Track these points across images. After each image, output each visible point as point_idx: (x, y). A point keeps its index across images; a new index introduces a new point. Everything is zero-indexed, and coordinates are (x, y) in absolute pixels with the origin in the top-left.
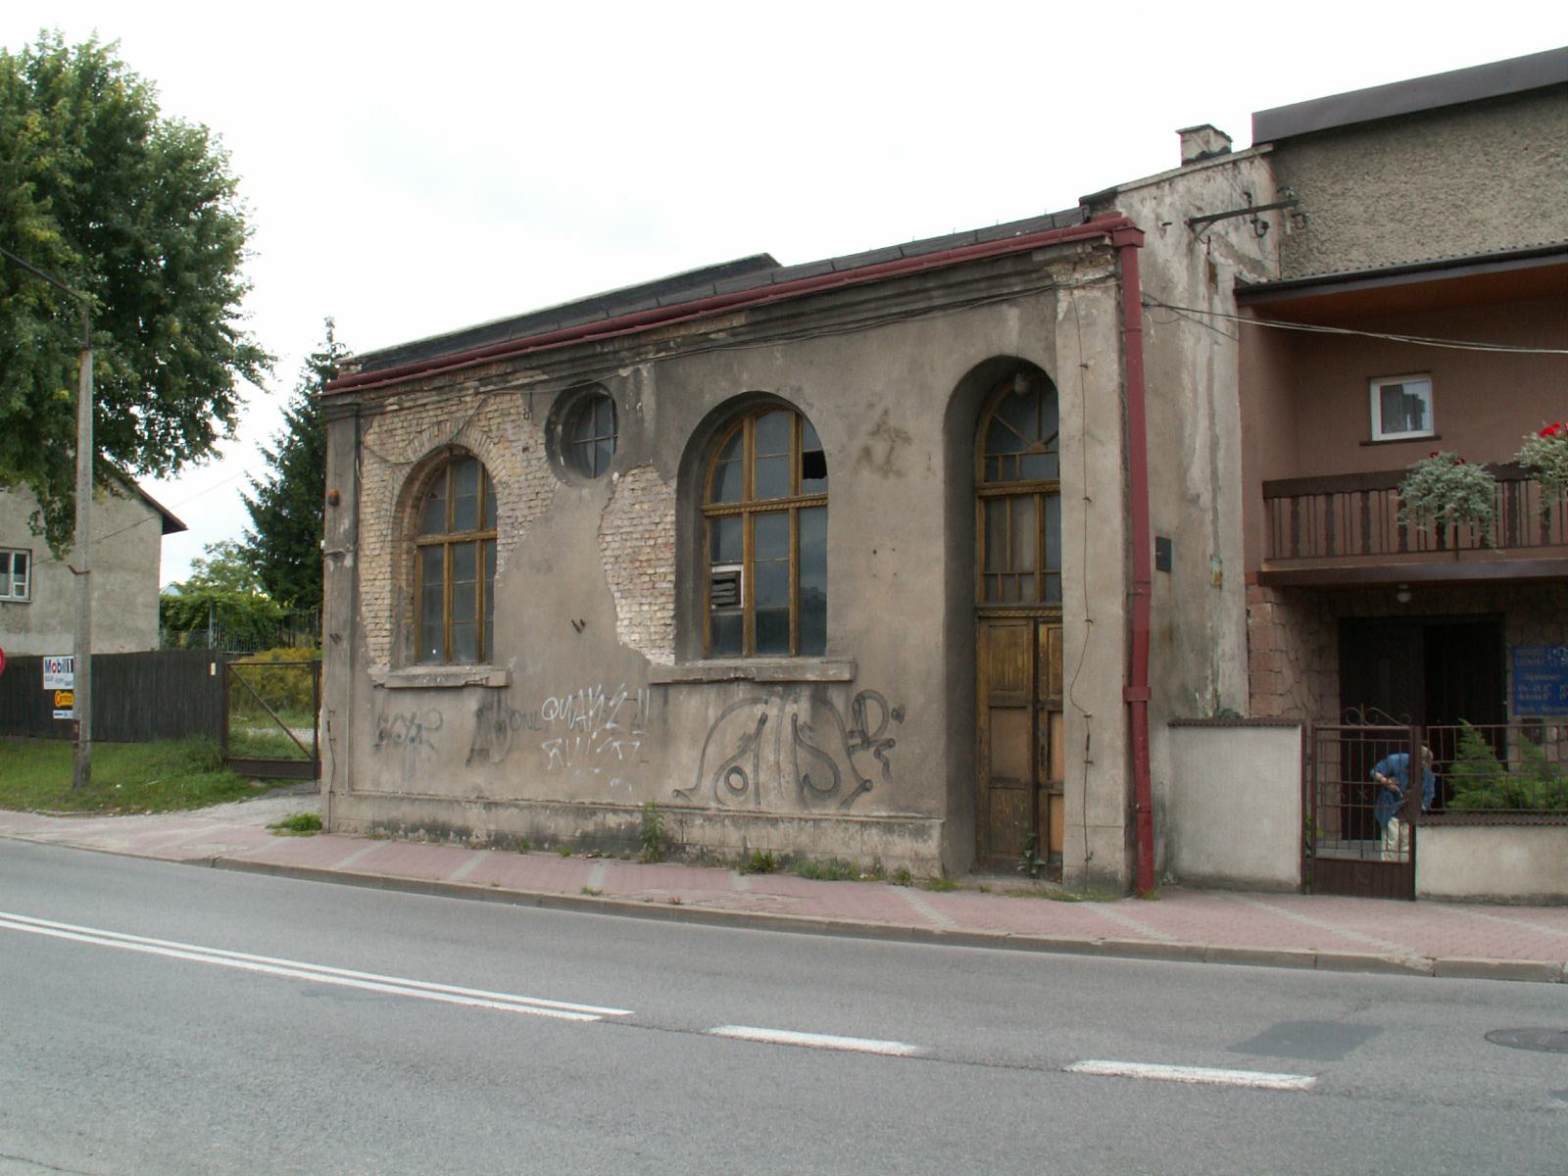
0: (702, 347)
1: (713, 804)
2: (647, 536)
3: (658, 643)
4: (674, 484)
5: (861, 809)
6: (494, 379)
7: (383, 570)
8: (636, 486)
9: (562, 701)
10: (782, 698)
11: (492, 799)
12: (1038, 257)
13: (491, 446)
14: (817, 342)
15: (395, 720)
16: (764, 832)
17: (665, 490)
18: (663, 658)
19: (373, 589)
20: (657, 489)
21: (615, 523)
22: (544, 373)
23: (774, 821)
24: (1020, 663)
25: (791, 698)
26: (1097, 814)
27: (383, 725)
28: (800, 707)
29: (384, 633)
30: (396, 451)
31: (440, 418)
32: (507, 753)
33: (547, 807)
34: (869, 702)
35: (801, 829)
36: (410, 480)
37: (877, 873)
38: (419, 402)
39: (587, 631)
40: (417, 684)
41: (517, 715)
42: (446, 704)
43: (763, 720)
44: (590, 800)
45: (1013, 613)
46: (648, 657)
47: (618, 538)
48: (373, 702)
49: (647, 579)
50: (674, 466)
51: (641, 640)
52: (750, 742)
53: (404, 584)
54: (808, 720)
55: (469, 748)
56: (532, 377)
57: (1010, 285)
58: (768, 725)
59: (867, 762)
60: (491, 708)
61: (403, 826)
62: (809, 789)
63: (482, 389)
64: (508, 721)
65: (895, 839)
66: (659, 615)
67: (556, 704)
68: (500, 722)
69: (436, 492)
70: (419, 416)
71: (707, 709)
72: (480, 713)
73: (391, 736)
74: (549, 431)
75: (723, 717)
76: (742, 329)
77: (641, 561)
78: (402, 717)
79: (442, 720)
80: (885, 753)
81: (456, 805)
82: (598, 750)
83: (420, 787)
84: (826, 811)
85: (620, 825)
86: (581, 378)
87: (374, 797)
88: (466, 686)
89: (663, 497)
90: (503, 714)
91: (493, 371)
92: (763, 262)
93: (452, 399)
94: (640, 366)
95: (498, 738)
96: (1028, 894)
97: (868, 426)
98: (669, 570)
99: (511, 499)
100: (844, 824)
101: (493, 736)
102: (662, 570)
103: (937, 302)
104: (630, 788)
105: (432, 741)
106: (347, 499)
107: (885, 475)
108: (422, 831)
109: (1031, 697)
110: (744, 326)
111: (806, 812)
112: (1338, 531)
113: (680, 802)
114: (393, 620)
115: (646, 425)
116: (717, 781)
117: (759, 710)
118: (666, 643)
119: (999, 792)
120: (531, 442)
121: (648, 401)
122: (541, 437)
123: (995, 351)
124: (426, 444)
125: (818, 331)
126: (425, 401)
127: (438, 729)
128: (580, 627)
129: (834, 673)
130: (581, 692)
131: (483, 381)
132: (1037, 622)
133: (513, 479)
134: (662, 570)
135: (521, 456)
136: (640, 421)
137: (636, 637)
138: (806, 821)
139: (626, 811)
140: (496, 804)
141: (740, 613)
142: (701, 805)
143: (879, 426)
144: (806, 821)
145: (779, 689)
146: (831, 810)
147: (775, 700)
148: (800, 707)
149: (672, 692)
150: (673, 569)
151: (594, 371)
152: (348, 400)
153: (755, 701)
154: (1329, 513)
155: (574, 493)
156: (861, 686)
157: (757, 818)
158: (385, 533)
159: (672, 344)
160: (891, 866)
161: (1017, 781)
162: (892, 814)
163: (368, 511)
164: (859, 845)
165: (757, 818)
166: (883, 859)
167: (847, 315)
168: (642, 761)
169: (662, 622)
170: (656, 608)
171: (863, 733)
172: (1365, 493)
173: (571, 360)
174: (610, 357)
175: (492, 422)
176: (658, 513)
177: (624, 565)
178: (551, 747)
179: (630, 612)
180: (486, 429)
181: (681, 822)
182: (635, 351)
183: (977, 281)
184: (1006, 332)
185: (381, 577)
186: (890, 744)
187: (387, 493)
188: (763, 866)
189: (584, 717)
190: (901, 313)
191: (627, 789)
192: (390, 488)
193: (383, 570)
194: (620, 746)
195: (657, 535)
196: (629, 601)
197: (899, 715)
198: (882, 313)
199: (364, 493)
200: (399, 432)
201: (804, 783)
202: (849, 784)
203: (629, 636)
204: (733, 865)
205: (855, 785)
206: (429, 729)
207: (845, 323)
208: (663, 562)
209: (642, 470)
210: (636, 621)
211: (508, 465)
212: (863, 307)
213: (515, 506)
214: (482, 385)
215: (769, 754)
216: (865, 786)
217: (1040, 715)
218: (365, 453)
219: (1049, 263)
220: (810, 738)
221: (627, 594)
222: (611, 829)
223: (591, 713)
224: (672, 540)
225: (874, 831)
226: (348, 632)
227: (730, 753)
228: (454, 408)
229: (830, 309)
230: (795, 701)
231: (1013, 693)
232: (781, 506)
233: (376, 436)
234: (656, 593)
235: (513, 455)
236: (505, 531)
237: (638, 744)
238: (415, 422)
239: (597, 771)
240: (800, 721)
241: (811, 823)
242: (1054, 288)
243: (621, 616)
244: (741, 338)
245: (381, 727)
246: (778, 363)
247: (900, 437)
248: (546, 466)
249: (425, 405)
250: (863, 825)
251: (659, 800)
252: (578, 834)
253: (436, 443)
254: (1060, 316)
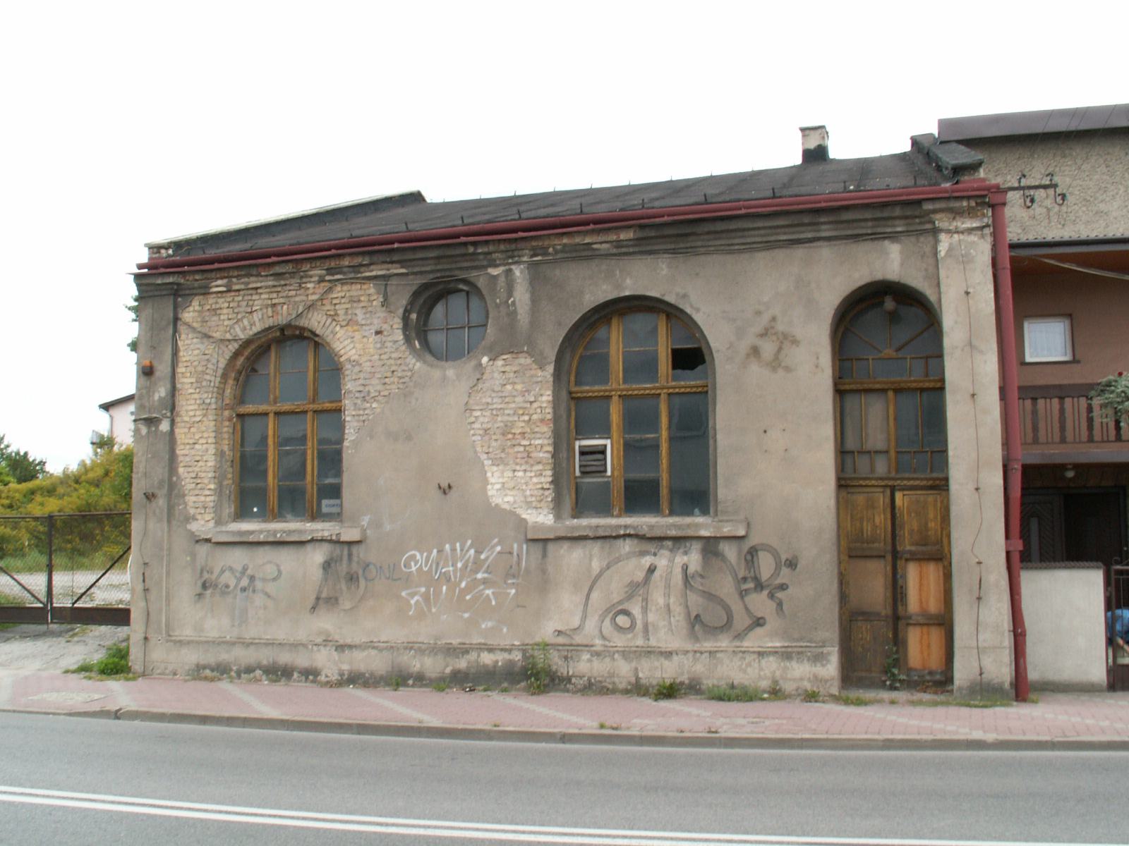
0: (584, 254)
1: (598, 642)
2: (521, 412)
3: (534, 504)
4: (550, 369)
6: (345, 270)
7: (205, 435)
8: (507, 369)
9: (425, 554)
10: (671, 551)
11: (341, 642)
12: (928, 206)
13: (338, 328)
14: (703, 258)
15: (223, 571)
16: (657, 664)
17: (540, 373)
18: (542, 518)
19: (193, 452)
20: (533, 372)
21: (484, 400)
22: (402, 267)
23: (668, 654)
24: (877, 521)
25: (681, 550)
26: (986, 637)
27: (206, 576)
28: (693, 558)
29: (208, 492)
30: (222, 328)
31: (274, 301)
32: (359, 601)
33: (411, 648)
34: (761, 554)
35: (695, 660)
36: (236, 355)
37: (776, 693)
38: (251, 286)
39: (453, 494)
40: (251, 538)
41: (371, 567)
42: (285, 557)
43: (652, 570)
44: (459, 640)
45: (874, 482)
46: (524, 516)
47: (488, 413)
48: (194, 556)
49: (522, 449)
50: (552, 355)
51: (515, 502)
53: (226, 448)
54: (699, 569)
55: (315, 596)
56: (388, 270)
57: (894, 226)
58: (657, 574)
59: (760, 603)
60: (341, 560)
61: (235, 668)
62: (697, 624)
63: (328, 278)
64: (360, 572)
65: (794, 664)
66: (535, 480)
67: (418, 557)
69: (256, 367)
70: (250, 297)
71: (591, 560)
72: (327, 566)
73: (216, 586)
74: (405, 319)
75: (608, 567)
76: (631, 243)
77: (515, 434)
78: (231, 569)
79: (280, 572)
80: (780, 595)
81: (301, 648)
82: (468, 597)
83: (251, 632)
84: (719, 644)
85: (497, 662)
86: (447, 274)
87: (198, 643)
88: (312, 540)
89: (539, 379)
90: (354, 566)
91: (346, 262)
92: (415, 198)
93: (291, 285)
94: (513, 267)
95: (349, 588)
96: (935, 704)
97: (758, 329)
98: (546, 442)
99: (362, 375)
100: (741, 654)
101: (344, 587)
102: (538, 442)
103: (824, 234)
104: (505, 630)
105: (268, 590)
106: (162, 369)
107: (774, 369)
108: (258, 672)
109: (889, 548)
110: (630, 240)
111: (698, 645)
112: (1042, 425)
113: (561, 640)
114: (216, 481)
115: (519, 317)
116: (603, 622)
117: (647, 561)
118: (543, 504)
119: (859, 624)
120: (385, 327)
121: (521, 295)
122: (397, 323)
123: (879, 276)
124: (258, 324)
125: (705, 249)
126: (259, 285)
127: (274, 579)
128: (445, 490)
129: (727, 530)
130: (447, 547)
131: (330, 271)
132: (893, 490)
133: (364, 359)
134: (538, 442)
135: (373, 338)
136: (513, 314)
137: (510, 499)
138: (701, 653)
139: (502, 650)
140: (350, 647)
141: (606, 480)
142: (585, 642)
143: (767, 330)
144: (701, 653)
145: (669, 543)
146: (724, 642)
147: (665, 553)
148: (693, 558)
149: (551, 547)
150: (551, 441)
151: (461, 269)
152: (171, 280)
153: (643, 553)
154: (1062, 411)
155: (436, 374)
156: (754, 540)
157: (649, 652)
158: (208, 401)
159: (551, 250)
160: (788, 687)
161: (878, 614)
162: (786, 645)
163: (186, 381)
164: (757, 671)
165: (649, 652)
166: (781, 682)
167: (734, 238)
168: (518, 606)
169: (540, 486)
170: (533, 474)
171: (756, 579)
172: (1061, 398)
173: (438, 258)
174: (481, 257)
175: (337, 307)
176: (532, 393)
177: (494, 437)
178: (412, 595)
179: (503, 477)
180: (332, 313)
181: (566, 658)
182: (510, 253)
183: (866, 220)
184: (891, 261)
185: (204, 441)
186: (783, 587)
187: (210, 366)
188: (669, 692)
189: (451, 569)
190: (786, 240)
191: (502, 630)
192: (215, 361)
193: (205, 435)
194: (493, 593)
195: (531, 412)
196: (501, 467)
197: (792, 564)
198: (772, 238)
199: (180, 365)
200: (225, 311)
202: (741, 621)
204: (626, 692)
205: (748, 622)
206: (264, 580)
207: (732, 245)
208: (538, 435)
209: (514, 356)
210: (511, 484)
211: (359, 346)
212: (756, 232)
213: (368, 382)
214: (328, 274)
215: (658, 598)
216: (759, 622)
217: (899, 562)
218: (182, 328)
219: (935, 211)
220: (702, 584)
221: (497, 462)
222: (487, 665)
223: (459, 565)
224: (549, 417)
225: (771, 658)
226: (165, 491)
227: (616, 598)
228: (294, 293)
229: (722, 232)
230: (686, 553)
231: (871, 545)
232: (653, 392)
233: (196, 314)
234: (532, 462)
235: (364, 337)
236: (355, 404)
237: (513, 591)
238: (244, 304)
239: (466, 615)
240: (691, 569)
241: (707, 654)
242: (935, 232)
243: (492, 480)
244: (624, 250)
245: (204, 579)
246: (664, 272)
247: (787, 339)
248: (404, 348)
249: (257, 288)
250: (761, 654)
252: (448, 670)
253: (269, 322)
254: (942, 254)
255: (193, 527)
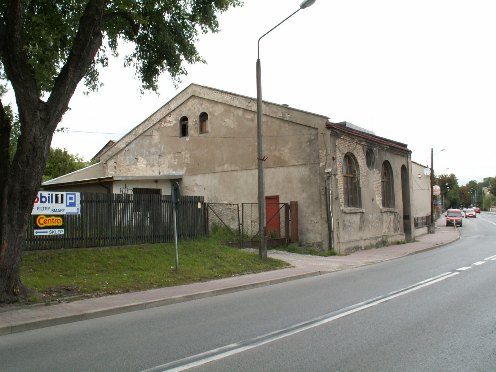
5: (399, 233)
18: (381, 207)
28: (393, 216)
52: (390, 222)
68: (363, 221)
72: (360, 218)
78: (348, 221)
113: (384, 234)
117: (390, 217)
121: (377, 156)
135: (362, 160)
136: (377, 160)
146: (396, 233)
197: (400, 217)
201: (394, 229)
203: (378, 203)
215: (391, 225)
242: (407, 157)
247: (398, 174)
249: (346, 140)
251: (383, 235)
255: (342, 208)
